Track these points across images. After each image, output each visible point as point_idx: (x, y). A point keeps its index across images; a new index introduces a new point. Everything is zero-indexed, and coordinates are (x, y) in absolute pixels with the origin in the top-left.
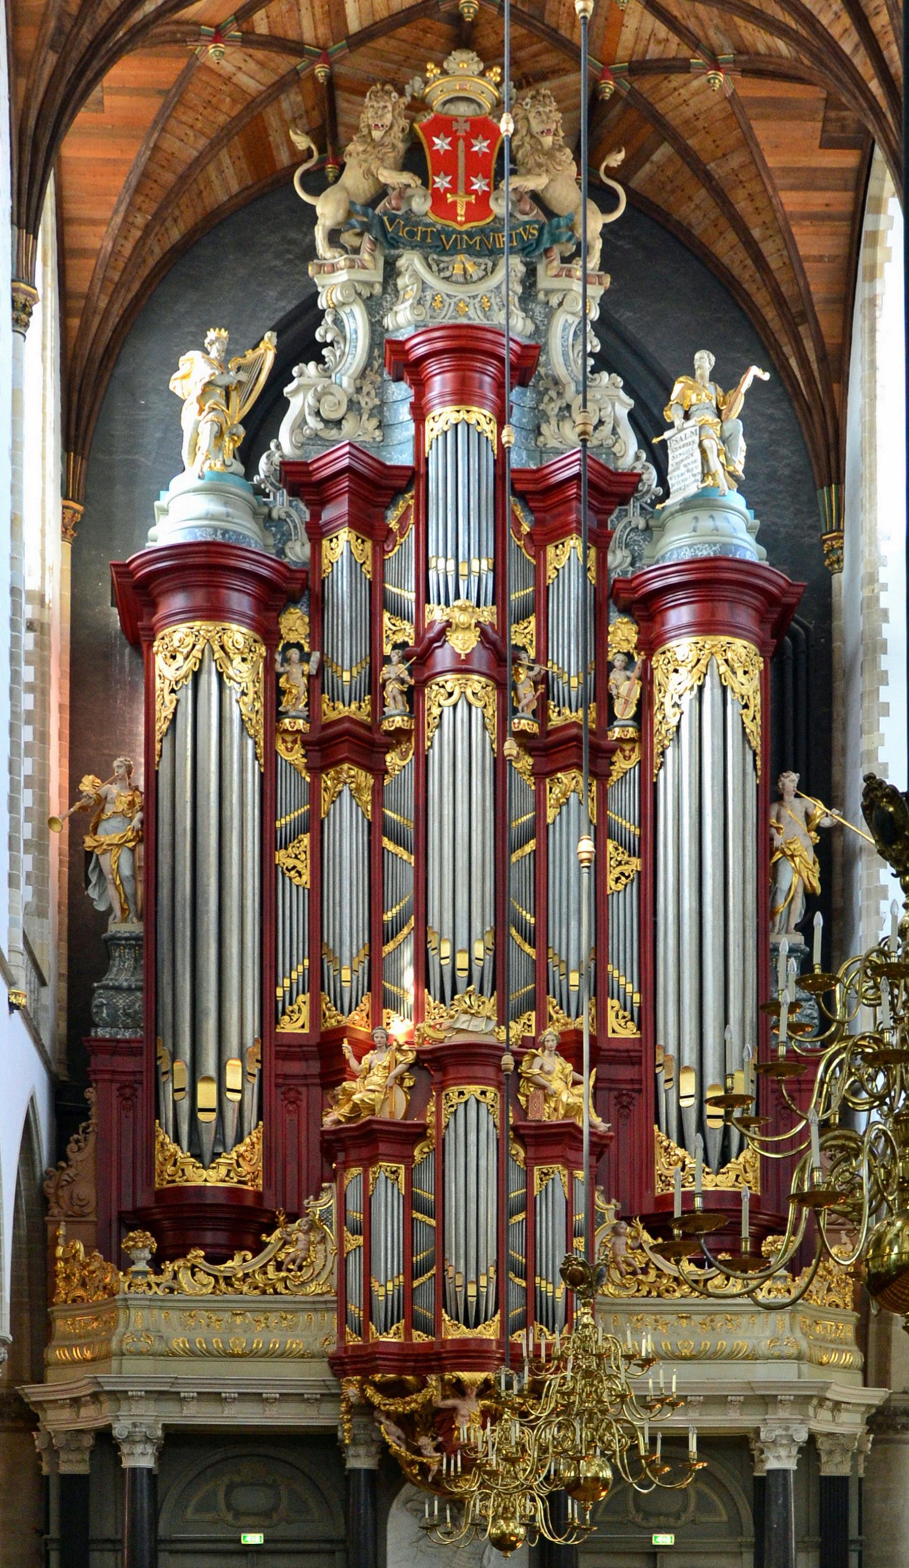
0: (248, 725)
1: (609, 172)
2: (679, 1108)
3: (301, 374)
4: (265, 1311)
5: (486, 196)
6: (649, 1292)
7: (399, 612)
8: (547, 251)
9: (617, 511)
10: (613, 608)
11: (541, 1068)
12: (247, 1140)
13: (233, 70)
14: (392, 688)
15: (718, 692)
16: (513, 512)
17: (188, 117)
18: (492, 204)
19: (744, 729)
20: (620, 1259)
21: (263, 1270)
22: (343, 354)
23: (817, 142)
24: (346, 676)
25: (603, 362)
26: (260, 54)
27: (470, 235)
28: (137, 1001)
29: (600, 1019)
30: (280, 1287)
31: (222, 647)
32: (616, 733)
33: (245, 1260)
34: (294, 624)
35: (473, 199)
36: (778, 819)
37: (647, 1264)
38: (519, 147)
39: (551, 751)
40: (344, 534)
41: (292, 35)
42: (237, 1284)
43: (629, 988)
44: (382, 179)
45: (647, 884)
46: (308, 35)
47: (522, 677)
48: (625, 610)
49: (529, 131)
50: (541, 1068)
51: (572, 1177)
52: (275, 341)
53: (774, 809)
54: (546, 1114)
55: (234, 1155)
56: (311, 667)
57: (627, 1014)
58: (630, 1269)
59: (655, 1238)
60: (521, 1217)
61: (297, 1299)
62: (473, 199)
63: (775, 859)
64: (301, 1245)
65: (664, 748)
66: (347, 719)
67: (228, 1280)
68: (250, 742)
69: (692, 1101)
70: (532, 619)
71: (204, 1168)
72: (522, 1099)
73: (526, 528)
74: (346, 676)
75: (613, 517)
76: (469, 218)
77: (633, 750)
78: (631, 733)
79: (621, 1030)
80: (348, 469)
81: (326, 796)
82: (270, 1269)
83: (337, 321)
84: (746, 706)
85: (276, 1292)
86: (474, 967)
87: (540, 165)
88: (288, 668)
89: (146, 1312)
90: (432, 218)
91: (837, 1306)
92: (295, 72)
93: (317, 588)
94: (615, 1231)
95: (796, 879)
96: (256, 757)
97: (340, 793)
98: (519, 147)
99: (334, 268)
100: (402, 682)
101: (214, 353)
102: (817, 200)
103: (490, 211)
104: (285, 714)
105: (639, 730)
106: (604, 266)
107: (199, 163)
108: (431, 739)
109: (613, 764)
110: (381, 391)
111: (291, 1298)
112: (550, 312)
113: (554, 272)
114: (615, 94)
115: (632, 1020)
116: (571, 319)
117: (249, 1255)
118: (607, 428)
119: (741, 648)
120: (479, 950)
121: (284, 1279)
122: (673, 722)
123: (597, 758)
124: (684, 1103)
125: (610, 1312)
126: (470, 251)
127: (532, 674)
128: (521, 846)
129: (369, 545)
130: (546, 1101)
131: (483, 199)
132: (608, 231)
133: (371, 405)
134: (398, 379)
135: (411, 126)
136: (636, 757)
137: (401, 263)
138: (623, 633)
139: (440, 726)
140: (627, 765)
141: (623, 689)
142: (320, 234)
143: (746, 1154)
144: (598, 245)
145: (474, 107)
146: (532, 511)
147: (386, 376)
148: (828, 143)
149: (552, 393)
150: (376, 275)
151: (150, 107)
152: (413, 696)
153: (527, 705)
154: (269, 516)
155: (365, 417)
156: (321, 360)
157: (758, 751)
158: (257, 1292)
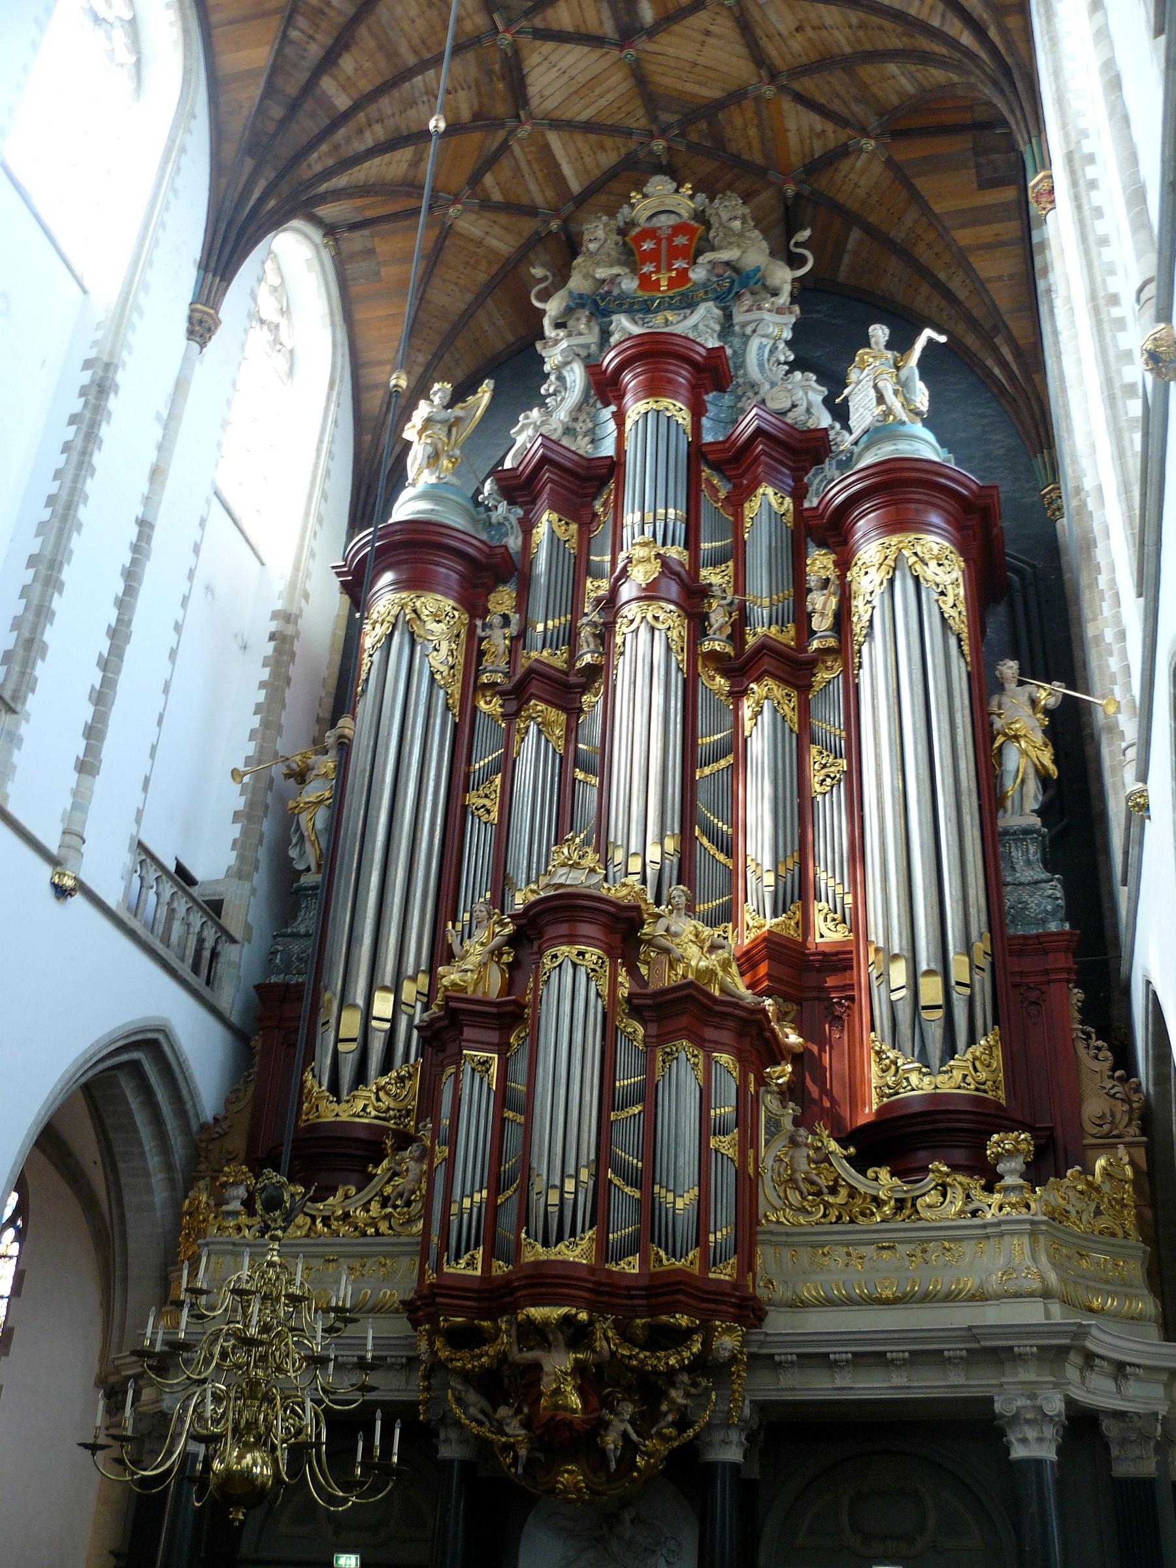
0: (438, 677)
1: (797, 245)
2: (892, 1005)
3: (527, 418)
4: (362, 1256)
5: (686, 270)
6: (839, 1217)
7: (599, 575)
8: (738, 295)
9: (813, 471)
10: (811, 544)
11: (667, 930)
12: (394, 1074)
13: (482, 235)
14: (585, 633)
15: (910, 583)
16: (708, 481)
17: (452, 275)
18: (692, 275)
19: (942, 613)
20: (800, 1176)
21: (366, 1208)
22: (562, 401)
23: (975, 186)
24: (540, 627)
25: (794, 366)
26: (502, 219)
27: (672, 298)
28: (309, 945)
29: (805, 924)
30: (383, 1227)
31: (415, 611)
32: (815, 644)
33: (347, 1197)
34: (503, 600)
35: (674, 274)
36: (1000, 708)
37: (836, 1181)
38: (715, 237)
39: (741, 668)
40: (545, 517)
41: (525, 200)
42: (335, 1225)
43: (839, 889)
44: (597, 276)
45: (853, 780)
46: (539, 200)
47: (715, 605)
48: (821, 544)
49: (721, 224)
50: (667, 930)
51: (709, 1060)
52: (492, 385)
53: (995, 701)
54: (669, 978)
55: (374, 1088)
56: (513, 630)
57: (838, 916)
58: (814, 1189)
59: (846, 1148)
60: (636, 1110)
61: (403, 1239)
62: (674, 274)
63: (997, 744)
64: (411, 1176)
65: (861, 645)
66: (537, 660)
67: (326, 1221)
68: (442, 692)
69: (903, 992)
70: (730, 563)
71: (338, 1102)
72: (644, 970)
73: (722, 495)
74: (540, 627)
75: (809, 475)
76: (671, 286)
77: (835, 660)
78: (832, 643)
79: (827, 932)
80: (544, 460)
81: (517, 738)
82: (375, 1207)
83: (561, 378)
84: (942, 593)
85: (377, 1234)
86: (649, 870)
87: (731, 243)
88: (488, 632)
89: (228, 1257)
90: (640, 293)
91: (1113, 1235)
92: (537, 233)
93: (526, 571)
94: (794, 1143)
95: (1023, 761)
96: (447, 708)
97: (528, 728)
98: (715, 237)
99: (556, 342)
100: (595, 625)
101: (437, 400)
102: (986, 233)
103: (689, 280)
104: (485, 671)
105: (840, 641)
106: (794, 299)
107: (468, 315)
108: (616, 667)
109: (814, 675)
110: (594, 418)
111: (395, 1240)
112: (746, 339)
113: (745, 308)
114: (798, 195)
115: (844, 922)
116: (765, 341)
117: (353, 1190)
118: (801, 409)
119: (934, 543)
120: (654, 853)
121: (388, 1217)
122: (866, 617)
123: (794, 668)
124: (895, 996)
125: (786, 1244)
126: (671, 307)
127: (723, 602)
128: (716, 761)
129: (574, 527)
130: (672, 967)
131: (683, 275)
132: (794, 280)
133: (584, 429)
134: (606, 404)
135: (625, 244)
136: (838, 668)
137: (613, 327)
138: (820, 563)
139: (622, 654)
140: (828, 676)
141: (818, 606)
142: (546, 322)
143: (977, 1050)
144: (787, 288)
145: (673, 216)
146: (729, 479)
147: (599, 405)
148: (986, 184)
149: (750, 394)
150: (591, 338)
151: (415, 269)
152: (605, 635)
153: (721, 628)
154: (490, 524)
155: (580, 438)
156: (543, 405)
157: (964, 636)
158: (357, 1233)
